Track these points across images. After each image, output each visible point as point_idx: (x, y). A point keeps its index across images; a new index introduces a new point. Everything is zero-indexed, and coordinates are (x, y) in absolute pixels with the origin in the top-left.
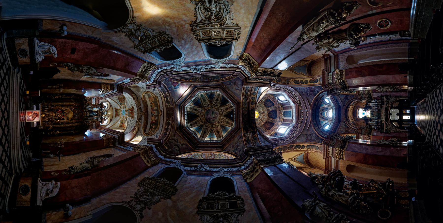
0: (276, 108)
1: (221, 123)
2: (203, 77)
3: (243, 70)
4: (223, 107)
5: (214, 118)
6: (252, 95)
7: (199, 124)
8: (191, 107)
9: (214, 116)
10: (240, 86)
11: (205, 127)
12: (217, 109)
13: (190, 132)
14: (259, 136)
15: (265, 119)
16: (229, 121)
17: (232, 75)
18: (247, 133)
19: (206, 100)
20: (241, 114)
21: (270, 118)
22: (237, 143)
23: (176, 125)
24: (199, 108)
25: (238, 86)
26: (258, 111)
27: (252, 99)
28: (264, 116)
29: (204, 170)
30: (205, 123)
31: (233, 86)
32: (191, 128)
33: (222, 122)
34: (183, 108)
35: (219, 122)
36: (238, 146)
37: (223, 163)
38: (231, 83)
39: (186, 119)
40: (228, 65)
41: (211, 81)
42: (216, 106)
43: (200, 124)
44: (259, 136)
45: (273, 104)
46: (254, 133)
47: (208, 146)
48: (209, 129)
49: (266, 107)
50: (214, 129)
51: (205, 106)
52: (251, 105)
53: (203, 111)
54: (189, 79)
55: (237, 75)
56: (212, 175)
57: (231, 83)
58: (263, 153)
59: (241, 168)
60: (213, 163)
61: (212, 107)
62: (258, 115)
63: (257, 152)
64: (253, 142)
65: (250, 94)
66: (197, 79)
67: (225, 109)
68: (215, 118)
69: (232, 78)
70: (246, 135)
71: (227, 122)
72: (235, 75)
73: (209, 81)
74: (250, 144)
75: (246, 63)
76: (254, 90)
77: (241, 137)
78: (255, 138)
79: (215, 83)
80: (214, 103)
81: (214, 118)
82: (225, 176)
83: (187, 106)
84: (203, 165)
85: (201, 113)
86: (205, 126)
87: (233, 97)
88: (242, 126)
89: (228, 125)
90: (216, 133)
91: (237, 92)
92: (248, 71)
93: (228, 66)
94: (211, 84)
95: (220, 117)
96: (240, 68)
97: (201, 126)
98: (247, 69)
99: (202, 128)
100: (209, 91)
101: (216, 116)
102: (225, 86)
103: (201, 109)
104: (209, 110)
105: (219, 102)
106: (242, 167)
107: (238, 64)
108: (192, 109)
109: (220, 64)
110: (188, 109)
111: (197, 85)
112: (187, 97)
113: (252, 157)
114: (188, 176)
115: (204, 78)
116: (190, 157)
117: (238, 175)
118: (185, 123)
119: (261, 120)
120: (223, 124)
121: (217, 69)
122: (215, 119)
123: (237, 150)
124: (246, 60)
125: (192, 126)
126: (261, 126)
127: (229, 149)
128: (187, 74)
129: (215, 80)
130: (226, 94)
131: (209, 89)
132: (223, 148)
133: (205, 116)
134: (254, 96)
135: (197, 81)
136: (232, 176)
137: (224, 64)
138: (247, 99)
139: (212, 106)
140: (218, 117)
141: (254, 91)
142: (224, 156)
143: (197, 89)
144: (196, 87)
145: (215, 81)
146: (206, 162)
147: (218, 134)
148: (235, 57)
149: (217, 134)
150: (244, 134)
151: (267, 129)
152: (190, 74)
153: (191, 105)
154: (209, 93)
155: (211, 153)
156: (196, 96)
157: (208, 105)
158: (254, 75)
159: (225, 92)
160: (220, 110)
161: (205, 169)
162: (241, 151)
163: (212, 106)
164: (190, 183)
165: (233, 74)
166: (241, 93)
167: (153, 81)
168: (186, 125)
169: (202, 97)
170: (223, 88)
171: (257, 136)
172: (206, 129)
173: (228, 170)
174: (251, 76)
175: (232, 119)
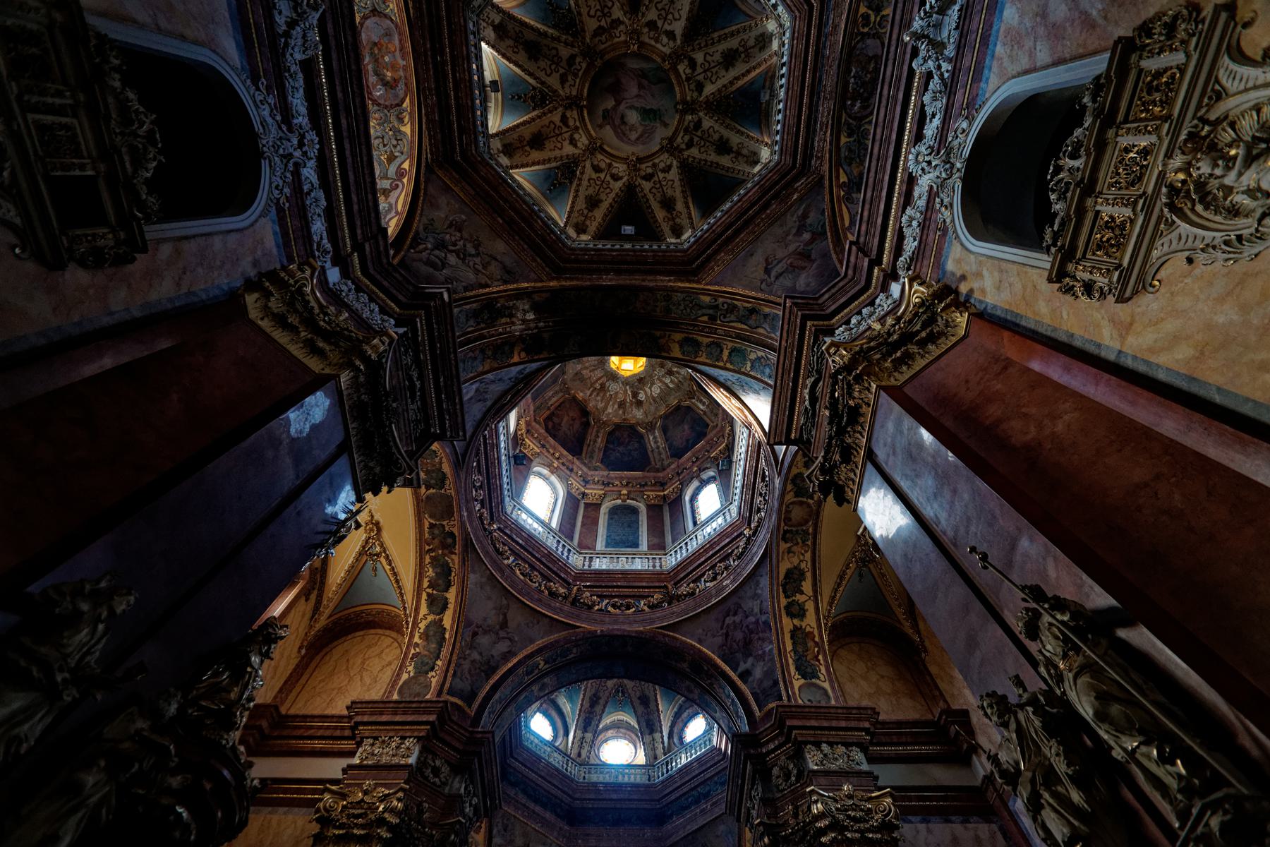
0: (658, 471)
1: (588, 164)
2: (877, 58)
3: (872, 304)
5: (623, 117)
6: (730, 345)
7: (584, 11)
9: (633, 117)
10: (786, 281)
11: (565, 52)
12: (671, 140)
14: (515, 370)
15: (606, 408)
16: (599, 214)
17: (851, 243)
18: (535, 308)
19: (733, 73)
20: (636, 280)
21: (611, 433)
22: (476, 247)
24: (684, 14)
25: (786, 271)
26: (646, 370)
27: (708, 346)
28: (622, 405)
29: (281, 21)
30: (589, 53)
31: (792, 248)
33: (597, 169)
35: (595, 148)
36: (463, 256)
37: (349, 160)
38: (806, 236)
40: (915, 223)
41: (841, 107)
42: (687, 138)
43: (585, 18)
44: (514, 370)
45: (677, 453)
46: (532, 344)
47: (444, 63)
48: (554, 81)
49: (666, 417)
50: (556, 118)
51: (693, 64)
52: (678, 337)
53: (665, 46)
55: (850, 272)
56: (255, 79)
57: (806, 236)
58: (422, 389)
59: (328, 265)
61: (683, 113)
62: (628, 374)
63: (426, 356)
64: (482, 337)
65: (738, 336)
67: (670, 192)
68: (621, 129)
69: (838, 242)
70: (523, 305)
72: (853, 259)
73: (843, 94)
74: (471, 322)
75: (910, 321)
76: (759, 359)
77: (509, 275)
78: (507, 348)
79: (824, 140)
80: (707, 123)
81: (617, 122)
82: (265, 165)
84: (314, 18)
85: (652, 25)
86: (573, 57)
87: (730, 240)
88: (568, 283)
89: (581, 204)
90: (533, 128)
91: (755, 267)
92: (862, 328)
93: (911, 219)
94: (825, 109)
95: (625, 160)
96: (885, 288)
98: (877, 326)
99: (554, 27)
100: (782, 94)
101: (634, 136)
102: (800, 199)
103: (678, 27)
104: (671, 89)
105: (713, 157)
106: (337, 269)
107: (911, 281)
113: (396, 326)
117: (287, 244)
119: (598, 386)
120: (586, 177)
121: (908, 152)
122: (614, 128)
123: (436, 247)
124: (932, 320)
126: (569, 384)
127: (443, 201)
129: (844, 140)
130: (753, 205)
131: (796, 97)
133: (635, 55)
134: (726, 353)
135: (863, 10)
136: (273, 210)
138: (713, 319)
139: (689, 107)
140: (627, 150)
141: (753, 356)
142: (392, 170)
145: (838, 139)
147: (527, 136)
148: (958, 261)
149: (527, 133)
151: (553, 414)
154: (773, 95)
155: (401, 86)
157: (700, 87)
158: (838, 359)
159: (760, 199)
160: (663, 160)
162: (431, 270)
163: (693, 112)
165: (859, 249)
166: (745, 287)
169: (751, 42)
171: (516, 359)
172: (557, 59)
173: (306, 188)
174: (833, 344)
175: (609, 231)
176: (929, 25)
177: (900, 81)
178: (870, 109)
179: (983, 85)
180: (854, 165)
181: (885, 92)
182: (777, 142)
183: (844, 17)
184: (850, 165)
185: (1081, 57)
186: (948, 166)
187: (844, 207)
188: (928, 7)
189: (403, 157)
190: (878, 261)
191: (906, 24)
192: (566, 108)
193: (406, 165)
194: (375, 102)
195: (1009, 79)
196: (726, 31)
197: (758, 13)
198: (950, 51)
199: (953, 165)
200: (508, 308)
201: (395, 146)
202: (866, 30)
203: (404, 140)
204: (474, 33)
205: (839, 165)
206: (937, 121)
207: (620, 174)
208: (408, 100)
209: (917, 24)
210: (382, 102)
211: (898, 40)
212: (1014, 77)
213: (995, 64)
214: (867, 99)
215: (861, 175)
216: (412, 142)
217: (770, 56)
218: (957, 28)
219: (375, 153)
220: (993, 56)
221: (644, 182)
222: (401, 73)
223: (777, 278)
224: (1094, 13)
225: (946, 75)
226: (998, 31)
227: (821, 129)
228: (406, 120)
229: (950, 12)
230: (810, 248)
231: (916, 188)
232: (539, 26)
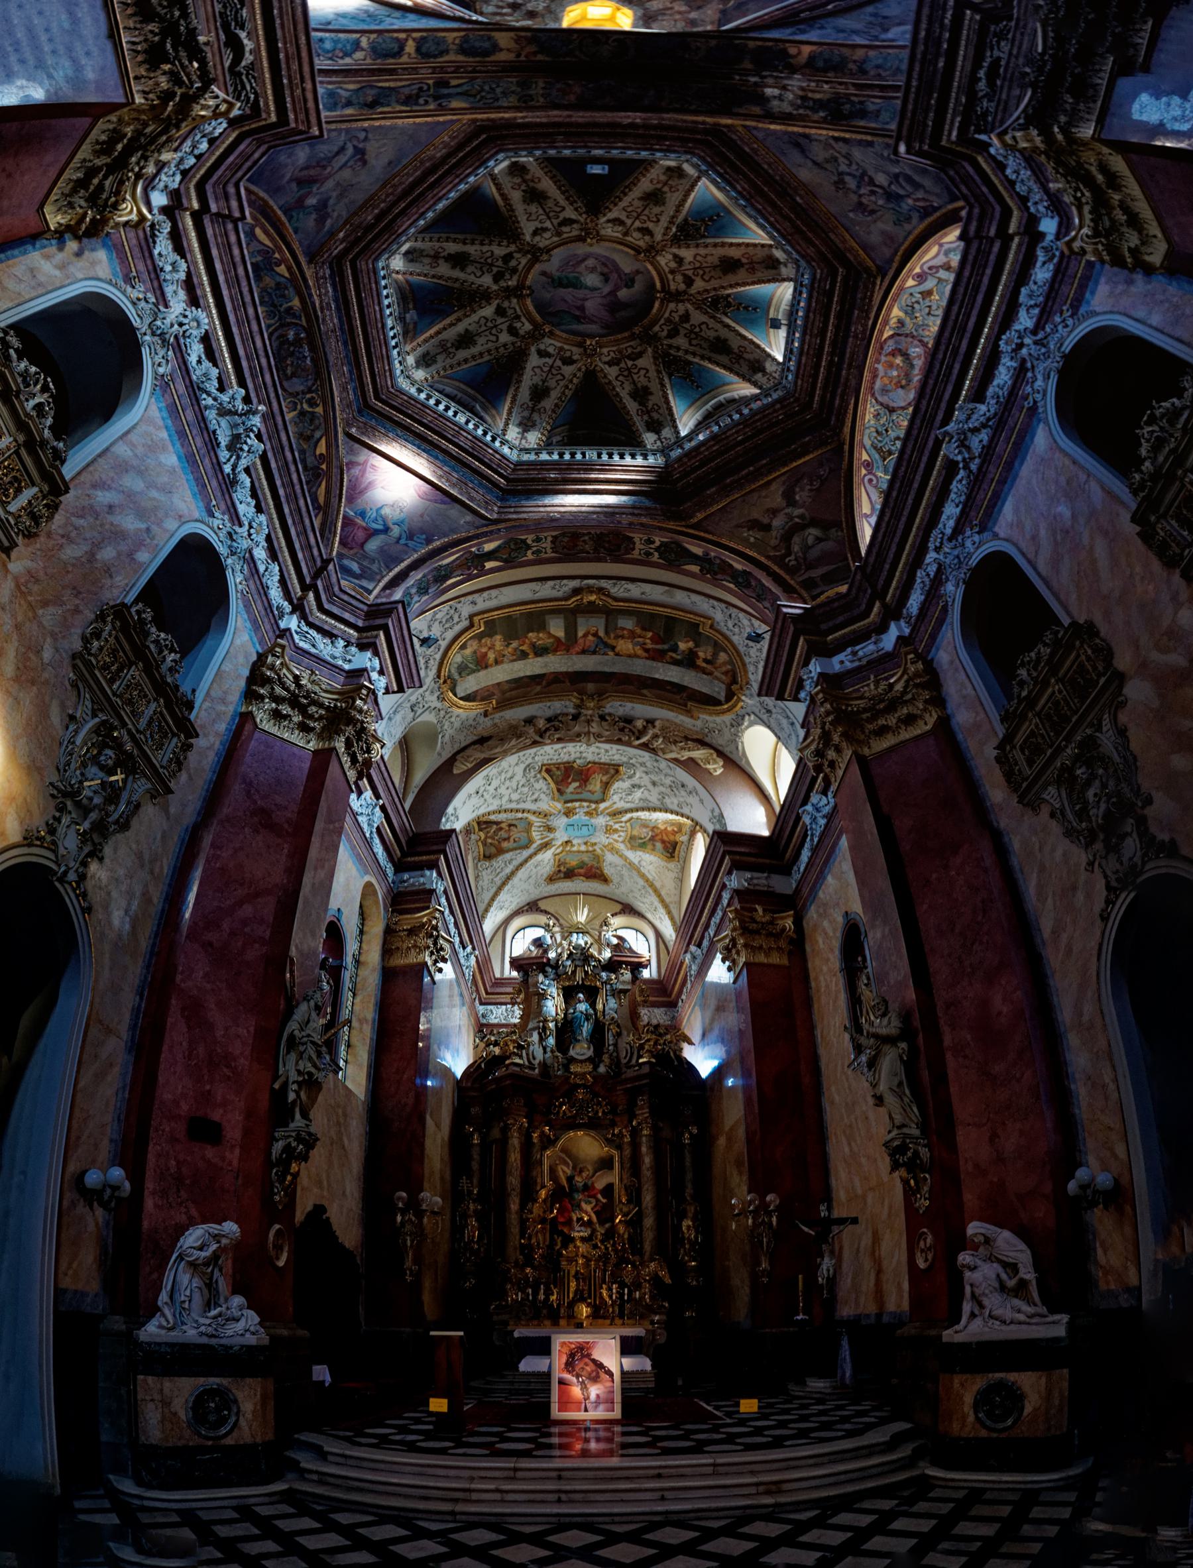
4: (522, 218)
8: (520, 425)
13: (702, 443)
16: (645, 184)
23: (644, 520)
25: (330, 160)
31: (330, 184)
32: (676, 427)
34: (521, 475)
39: (605, 457)
43: (652, 368)
54: (310, 461)
57: (312, 201)
60: (957, 366)
66: (302, 413)
71: (654, 198)
73: (313, 339)
83: (506, 450)
97: (667, 365)
108: (536, 416)
109: (168, 321)
110: (533, 438)
111: (349, 406)
112: (445, 452)
114: (996, 529)
115: (289, 372)
116: (880, 474)
118: (639, 461)
123: (899, 198)
125: (660, 421)
128: (278, 483)
129: (296, 303)
131: (372, 325)
132: (867, 270)
137: (169, 295)
143: (377, 398)
144: (365, 407)
146: (939, 399)
150: (771, 117)
152: (273, 465)
153: (501, 426)
155: (890, 346)
156: (429, 397)
161: (984, 426)
164: (1034, 538)
167: (369, 654)
168: (651, 460)
170: (358, 240)
176: (243, 423)
177: (252, 374)
178: (273, 338)
179: (163, 405)
180: (273, 285)
181: (264, 361)
182: (384, 278)
183: (337, 400)
184: (278, 284)
185: (88, 465)
186: (159, 332)
187: (267, 242)
188: (252, 435)
189: (912, 290)
190: (197, 217)
191: (268, 417)
192: (685, 292)
193: (910, 282)
194: (925, 345)
195: (140, 420)
196: (474, 363)
197: (438, 382)
198: (211, 415)
199: (153, 334)
200: (806, 108)
201: (918, 302)
202: (308, 396)
203: (904, 304)
204: (788, 369)
205: (293, 280)
206: (193, 359)
207: (610, 225)
208: (886, 335)
209: (256, 421)
210: (916, 342)
211: (270, 403)
212: (136, 424)
213: (161, 423)
214: (281, 344)
215: (258, 278)
216: (894, 300)
217: (413, 350)
218: (214, 432)
219: (944, 303)
220: (166, 427)
221: (573, 217)
222: (883, 358)
223: (342, 149)
224: (100, 493)
225: (204, 396)
226: (173, 445)
227: (328, 304)
228: (895, 320)
229: (228, 439)
230: (302, 192)
231: (185, 298)
232: (710, 366)
